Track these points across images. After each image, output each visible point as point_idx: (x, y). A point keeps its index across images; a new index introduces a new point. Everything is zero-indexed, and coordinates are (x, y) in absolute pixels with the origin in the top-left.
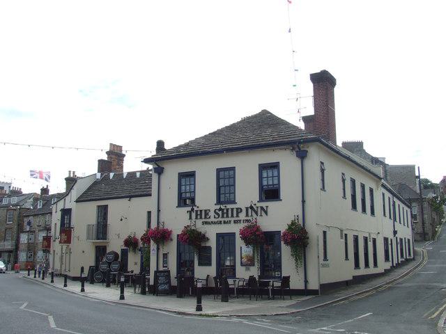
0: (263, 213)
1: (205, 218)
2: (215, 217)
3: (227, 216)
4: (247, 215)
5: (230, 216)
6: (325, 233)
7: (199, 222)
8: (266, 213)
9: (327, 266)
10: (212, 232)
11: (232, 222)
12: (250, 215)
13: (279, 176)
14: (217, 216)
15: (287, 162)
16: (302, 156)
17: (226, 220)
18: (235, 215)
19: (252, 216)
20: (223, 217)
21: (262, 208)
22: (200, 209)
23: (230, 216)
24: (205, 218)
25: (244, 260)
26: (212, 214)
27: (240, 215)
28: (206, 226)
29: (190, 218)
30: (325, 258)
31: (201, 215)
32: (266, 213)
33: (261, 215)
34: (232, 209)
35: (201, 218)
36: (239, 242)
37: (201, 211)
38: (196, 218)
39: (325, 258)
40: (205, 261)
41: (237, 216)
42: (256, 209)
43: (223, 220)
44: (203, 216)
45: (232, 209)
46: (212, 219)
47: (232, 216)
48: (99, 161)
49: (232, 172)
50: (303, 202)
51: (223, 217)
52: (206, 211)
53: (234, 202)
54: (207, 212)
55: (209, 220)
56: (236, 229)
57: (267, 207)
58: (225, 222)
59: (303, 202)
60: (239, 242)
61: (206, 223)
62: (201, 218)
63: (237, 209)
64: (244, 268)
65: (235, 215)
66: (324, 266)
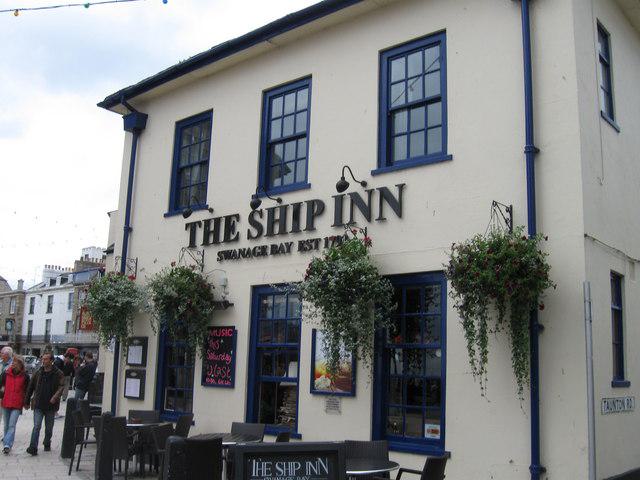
0: (389, 212)
1: (227, 240)
2: (250, 237)
3: (283, 232)
4: (338, 223)
6: (617, 280)
7: (212, 253)
9: (625, 406)
10: (237, 282)
11: (295, 247)
12: (346, 219)
13: (443, 70)
14: (255, 233)
17: (279, 241)
19: (352, 222)
21: (385, 194)
22: (217, 214)
26: (243, 227)
27: (319, 223)
28: (228, 265)
29: (192, 244)
30: (619, 379)
31: (271, 222)
32: (398, 209)
33: (381, 219)
35: (216, 242)
37: (218, 221)
38: (206, 243)
39: (619, 379)
40: (220, 376)
41: (311, 228)
42: (365, 197)
45: (297, 207)
46: (245, 244)
47: (296, 230)
50: (532, 152)
51: (271, 234)
52: (228, 219)
53: (306, 186)
54: (231, 222)
57: (401, 187)
59: (532, 152)
60: (312, 320)
63: (311, 204)
64: (321, 402)
66: (611, 406)
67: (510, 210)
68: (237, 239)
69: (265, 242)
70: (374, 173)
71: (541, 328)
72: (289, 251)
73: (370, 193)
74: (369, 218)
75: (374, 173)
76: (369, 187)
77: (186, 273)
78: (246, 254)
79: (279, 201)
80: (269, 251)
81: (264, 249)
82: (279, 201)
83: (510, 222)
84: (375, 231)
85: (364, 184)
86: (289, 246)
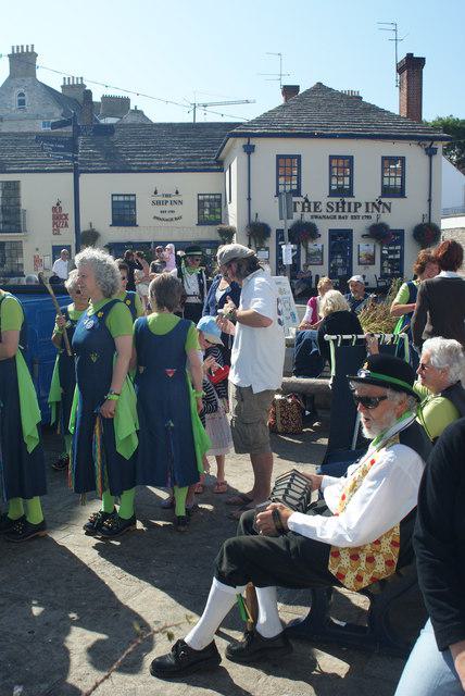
0: (386, 210)
3: (343, 211)
8: (389, 210)
16: (431, 152)
17: (342, 214)
18: (353, 209)
20: (338, 211)
21: (385, 204)
24: (315, 211)
25: (363, 259)
26: (323, 207)
32: (389, 210)
34: (350, 204)
38: (303, 211)
41: (356, 211)
43: (338, 214)
44: (312, 209)
45: (350, 204)
46: (324, 213)
47: (349, 211)
52: (315, 203)
55: (320, 214)
58: (340, 217)
60: (357, 240)
62: (309, 211)
63: (356, 204)
65: (353, 209)
69: (334, 213)
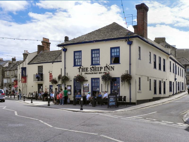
0: (112, 69)
1: (86, 71)
2: (90, 71)
3: (96, 71)
4: (105, 70)
5: (97, 70)
6: (140, 78)
7: (83, 73)
10: (89, 77)
11: (98, 73)
12: (106, 70)
13: (119, 52)
14: (91, 70)
15: (123, 46)
16: (130, 43)
17: (95, 72)
18: (99, 70)
19: (107, 70)
20: (94, 71)
21: (111, 67)
23: (97, 70)
24: (86, 71)
26: (89, 69)
27: (101, 70)
28: (86, 75)
29: (79, 71)
32: (113, 69)
34: (98, 68)
35: (84, 71)
36: (101, 82)
37: (84, 68)
38: (82, 71)
39: (140, 89)
41: (100, 70)
42: (109, 67)
43: (94, 72)
44: (85, 71)
45: (98, 68)
46: (89, 72)
47: (98, 70)
48: (38, 46)
49: (98, 51)
50: (130, 64)
51: (94, 71)
52: (86, 68)
53: (99, 64)
54: (87, 69)
56: (99, 76)
57: (114, 67)
58: (95, 73)
59: (130, 64)
61: (86, 73)
62: (84, 71)
63: (100, 67)
65: (99, 70)
66: (138, 92)
67: (127, 71)
68: (88, 71)
70: (110, 64)
71: (131, 84)
72: (97, 73)
73: (109, 67)
74: (109, 70)
75: (110, 64)
76: (109, 66)
77: (80, 75)
78: (89, 73)
79: (95, 66)
80: (94, 73)
81: (93, 73)
82: (95, 66)
83: (127, 72)
84: (110, 72)
85: (108, 65)
86: (97, 73)
